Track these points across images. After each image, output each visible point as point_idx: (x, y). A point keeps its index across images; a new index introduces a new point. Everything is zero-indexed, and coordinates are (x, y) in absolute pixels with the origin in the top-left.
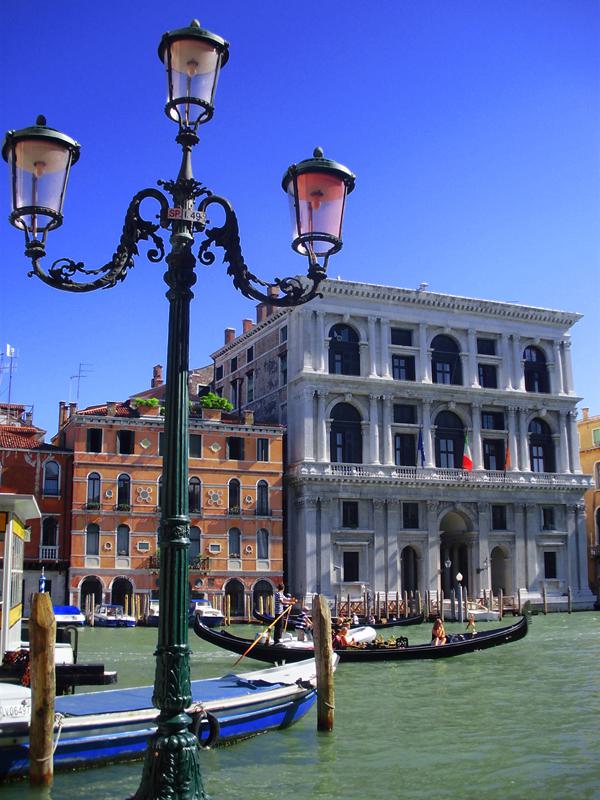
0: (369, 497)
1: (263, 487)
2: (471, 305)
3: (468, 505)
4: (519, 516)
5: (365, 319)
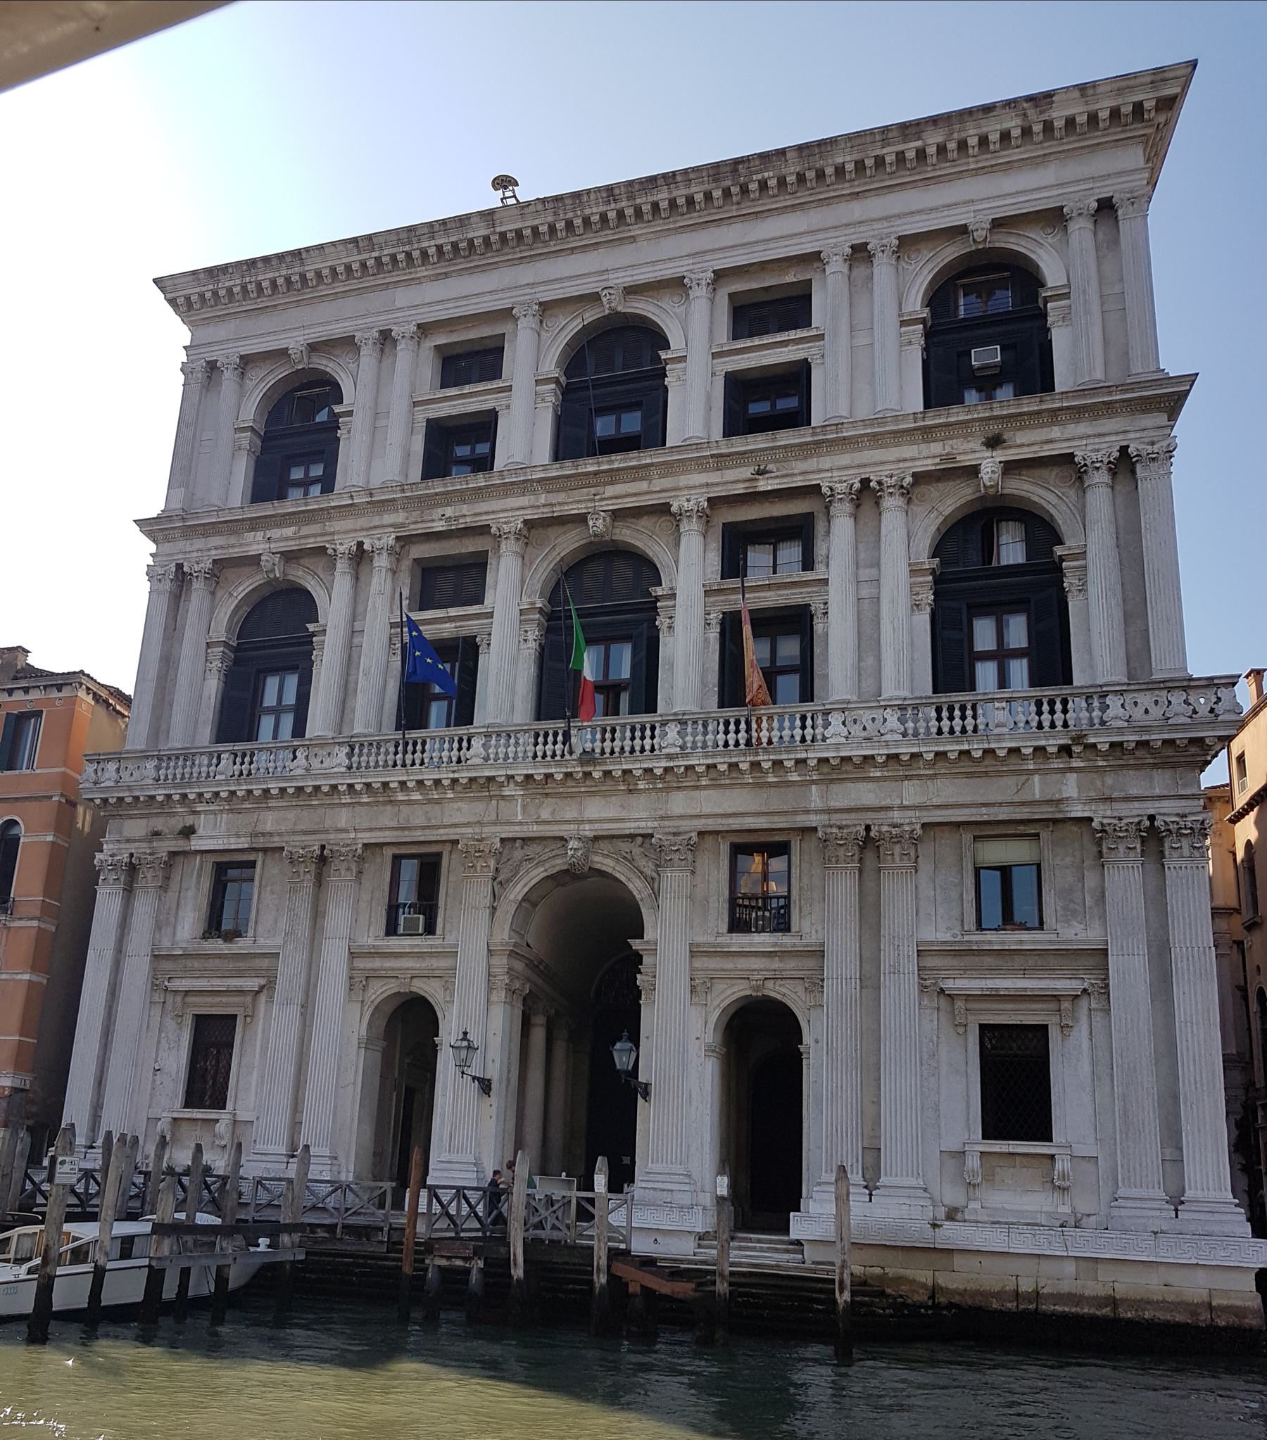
0: (276, 841)
2: (680, 193)
3: (624, 846)
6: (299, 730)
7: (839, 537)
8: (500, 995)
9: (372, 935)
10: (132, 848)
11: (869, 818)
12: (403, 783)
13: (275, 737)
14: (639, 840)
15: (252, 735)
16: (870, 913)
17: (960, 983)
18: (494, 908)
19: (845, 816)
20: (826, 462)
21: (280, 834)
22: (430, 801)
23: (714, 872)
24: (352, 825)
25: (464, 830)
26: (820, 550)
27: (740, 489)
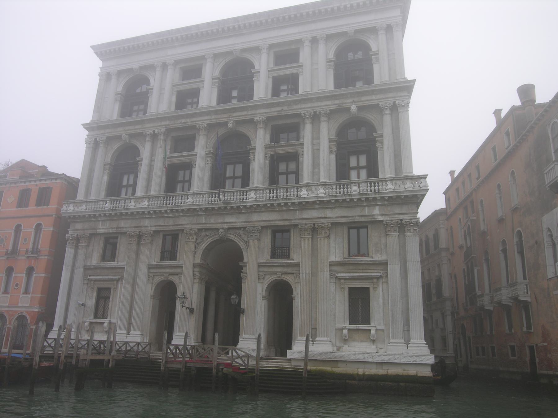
0: (124, 230)
1: (39, 227)
3: (238, 231)
4: (306, 244)
5: (152, 67)
6: (134, 193)
7: (307, 131)
8: (197, 281)
9: (155, 261)
10: (79, 232)
11: (314, 221)
12: (166, 211)
13: (126, 195)
14: (242, 229)
15: (119, 194)
16: (314, 251)
17: (342, 275)
18: (195, 252)
19: (307, 221)
20: (303, 106)
21: (126, 228)
22: (175, 217)
23: (267, 240)
24: (150, 225)
25: (186, 226)
26: (301, 134)
27: (276, 114)
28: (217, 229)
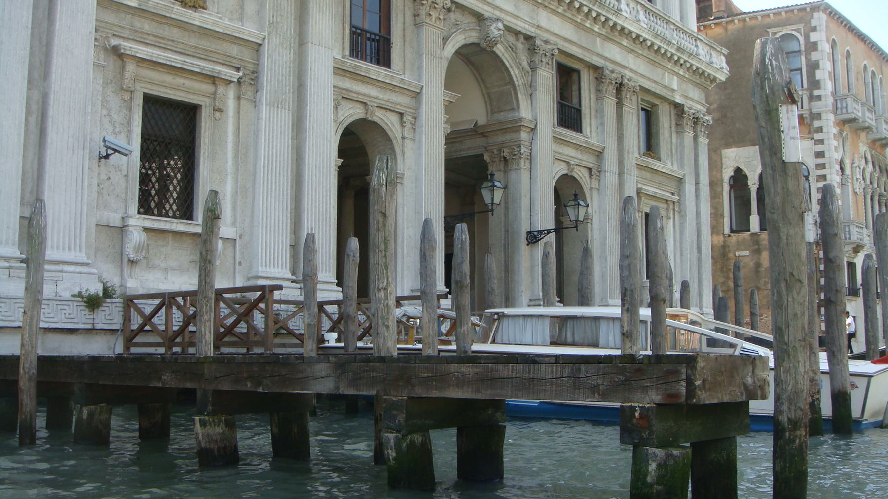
3: (511, 39)
28: (479, 18)
